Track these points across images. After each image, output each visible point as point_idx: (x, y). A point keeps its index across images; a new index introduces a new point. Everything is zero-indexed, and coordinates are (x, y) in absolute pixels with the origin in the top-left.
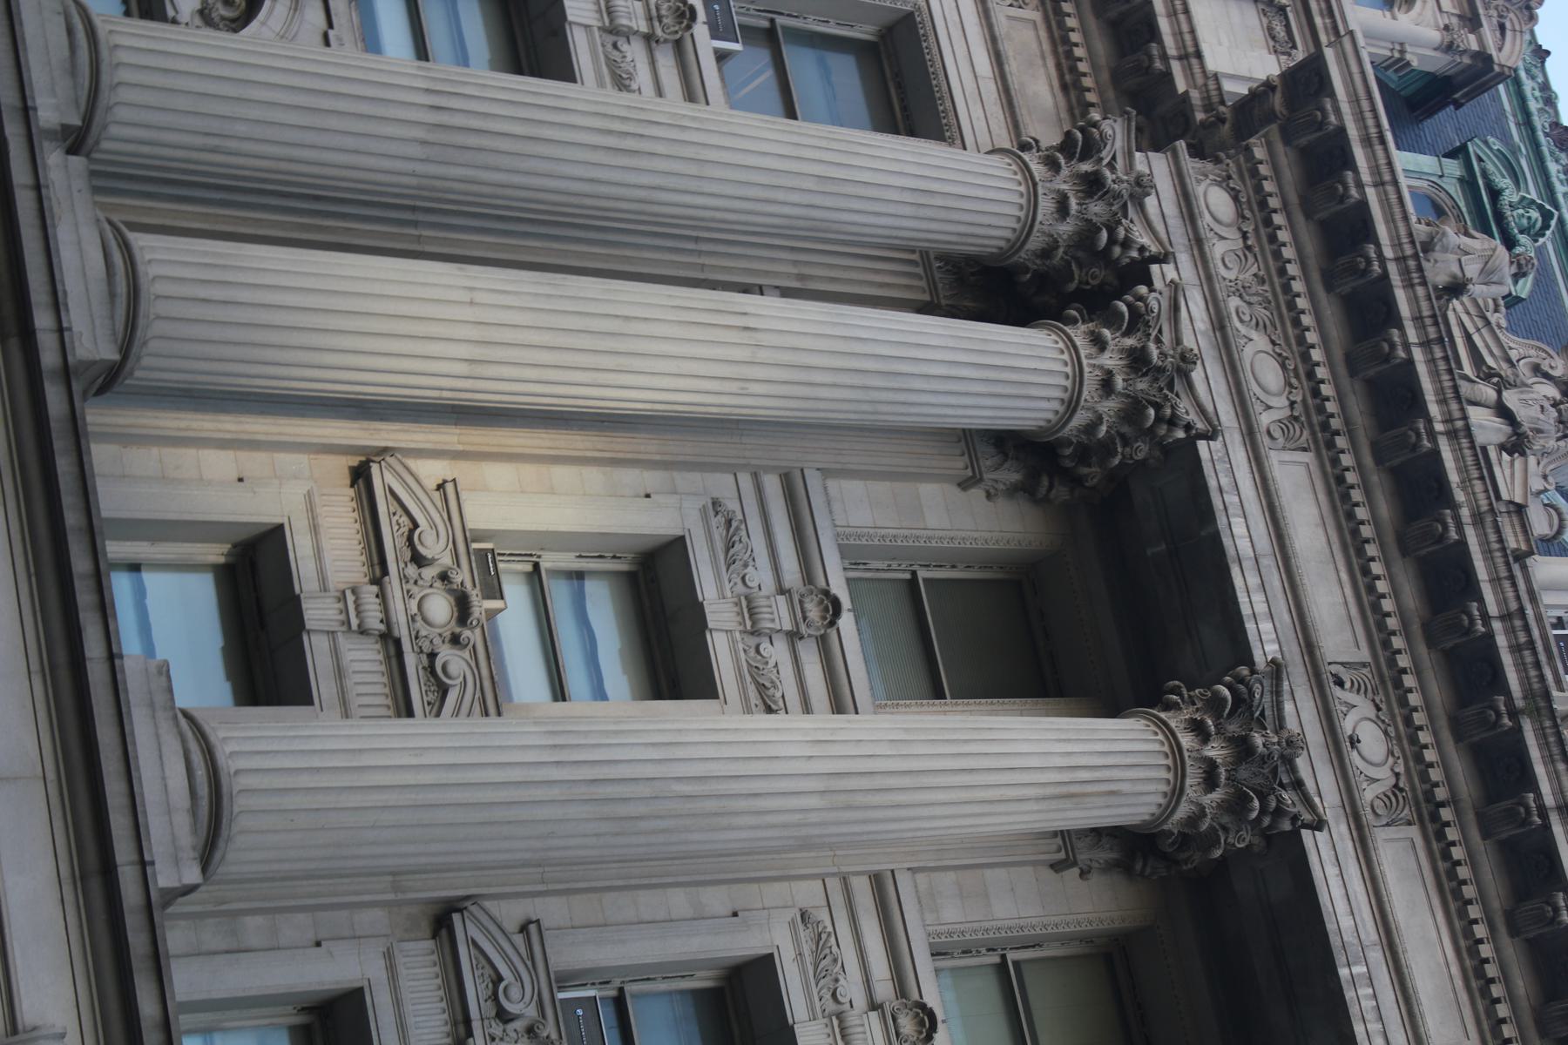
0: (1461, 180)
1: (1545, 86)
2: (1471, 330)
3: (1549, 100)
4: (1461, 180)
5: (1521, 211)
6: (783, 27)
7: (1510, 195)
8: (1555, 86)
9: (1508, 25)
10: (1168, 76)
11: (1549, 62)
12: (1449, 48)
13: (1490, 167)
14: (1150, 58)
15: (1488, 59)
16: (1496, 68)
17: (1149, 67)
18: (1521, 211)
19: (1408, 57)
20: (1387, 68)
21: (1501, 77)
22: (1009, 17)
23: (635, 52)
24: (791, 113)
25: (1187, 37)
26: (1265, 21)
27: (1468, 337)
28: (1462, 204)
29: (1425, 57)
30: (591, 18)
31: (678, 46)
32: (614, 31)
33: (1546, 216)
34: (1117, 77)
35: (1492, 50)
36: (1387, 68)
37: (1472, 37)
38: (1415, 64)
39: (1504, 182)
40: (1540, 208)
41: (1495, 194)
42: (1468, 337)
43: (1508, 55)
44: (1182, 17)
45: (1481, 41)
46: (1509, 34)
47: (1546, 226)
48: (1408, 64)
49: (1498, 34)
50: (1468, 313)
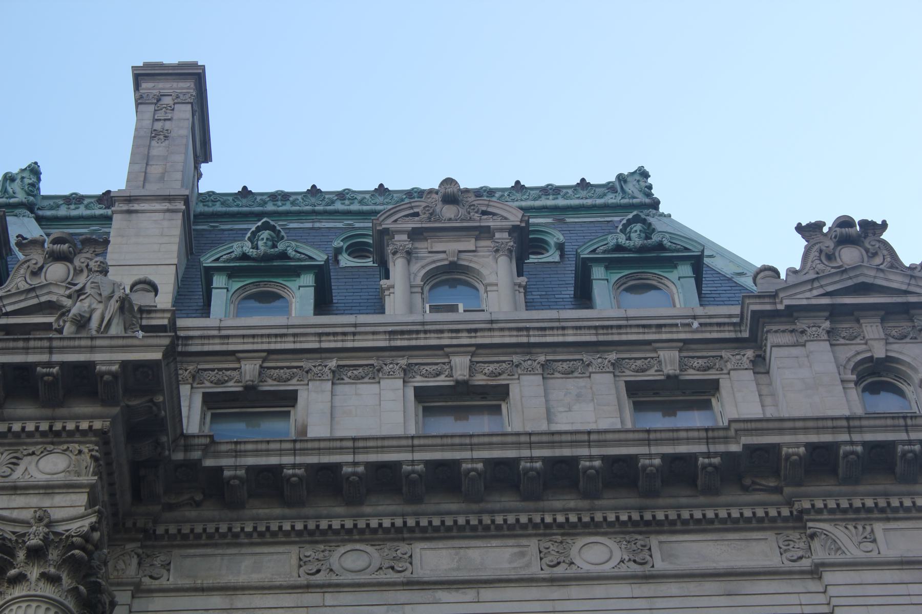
25: (696, 434)
26: (557, 375)
39: (611, 240)
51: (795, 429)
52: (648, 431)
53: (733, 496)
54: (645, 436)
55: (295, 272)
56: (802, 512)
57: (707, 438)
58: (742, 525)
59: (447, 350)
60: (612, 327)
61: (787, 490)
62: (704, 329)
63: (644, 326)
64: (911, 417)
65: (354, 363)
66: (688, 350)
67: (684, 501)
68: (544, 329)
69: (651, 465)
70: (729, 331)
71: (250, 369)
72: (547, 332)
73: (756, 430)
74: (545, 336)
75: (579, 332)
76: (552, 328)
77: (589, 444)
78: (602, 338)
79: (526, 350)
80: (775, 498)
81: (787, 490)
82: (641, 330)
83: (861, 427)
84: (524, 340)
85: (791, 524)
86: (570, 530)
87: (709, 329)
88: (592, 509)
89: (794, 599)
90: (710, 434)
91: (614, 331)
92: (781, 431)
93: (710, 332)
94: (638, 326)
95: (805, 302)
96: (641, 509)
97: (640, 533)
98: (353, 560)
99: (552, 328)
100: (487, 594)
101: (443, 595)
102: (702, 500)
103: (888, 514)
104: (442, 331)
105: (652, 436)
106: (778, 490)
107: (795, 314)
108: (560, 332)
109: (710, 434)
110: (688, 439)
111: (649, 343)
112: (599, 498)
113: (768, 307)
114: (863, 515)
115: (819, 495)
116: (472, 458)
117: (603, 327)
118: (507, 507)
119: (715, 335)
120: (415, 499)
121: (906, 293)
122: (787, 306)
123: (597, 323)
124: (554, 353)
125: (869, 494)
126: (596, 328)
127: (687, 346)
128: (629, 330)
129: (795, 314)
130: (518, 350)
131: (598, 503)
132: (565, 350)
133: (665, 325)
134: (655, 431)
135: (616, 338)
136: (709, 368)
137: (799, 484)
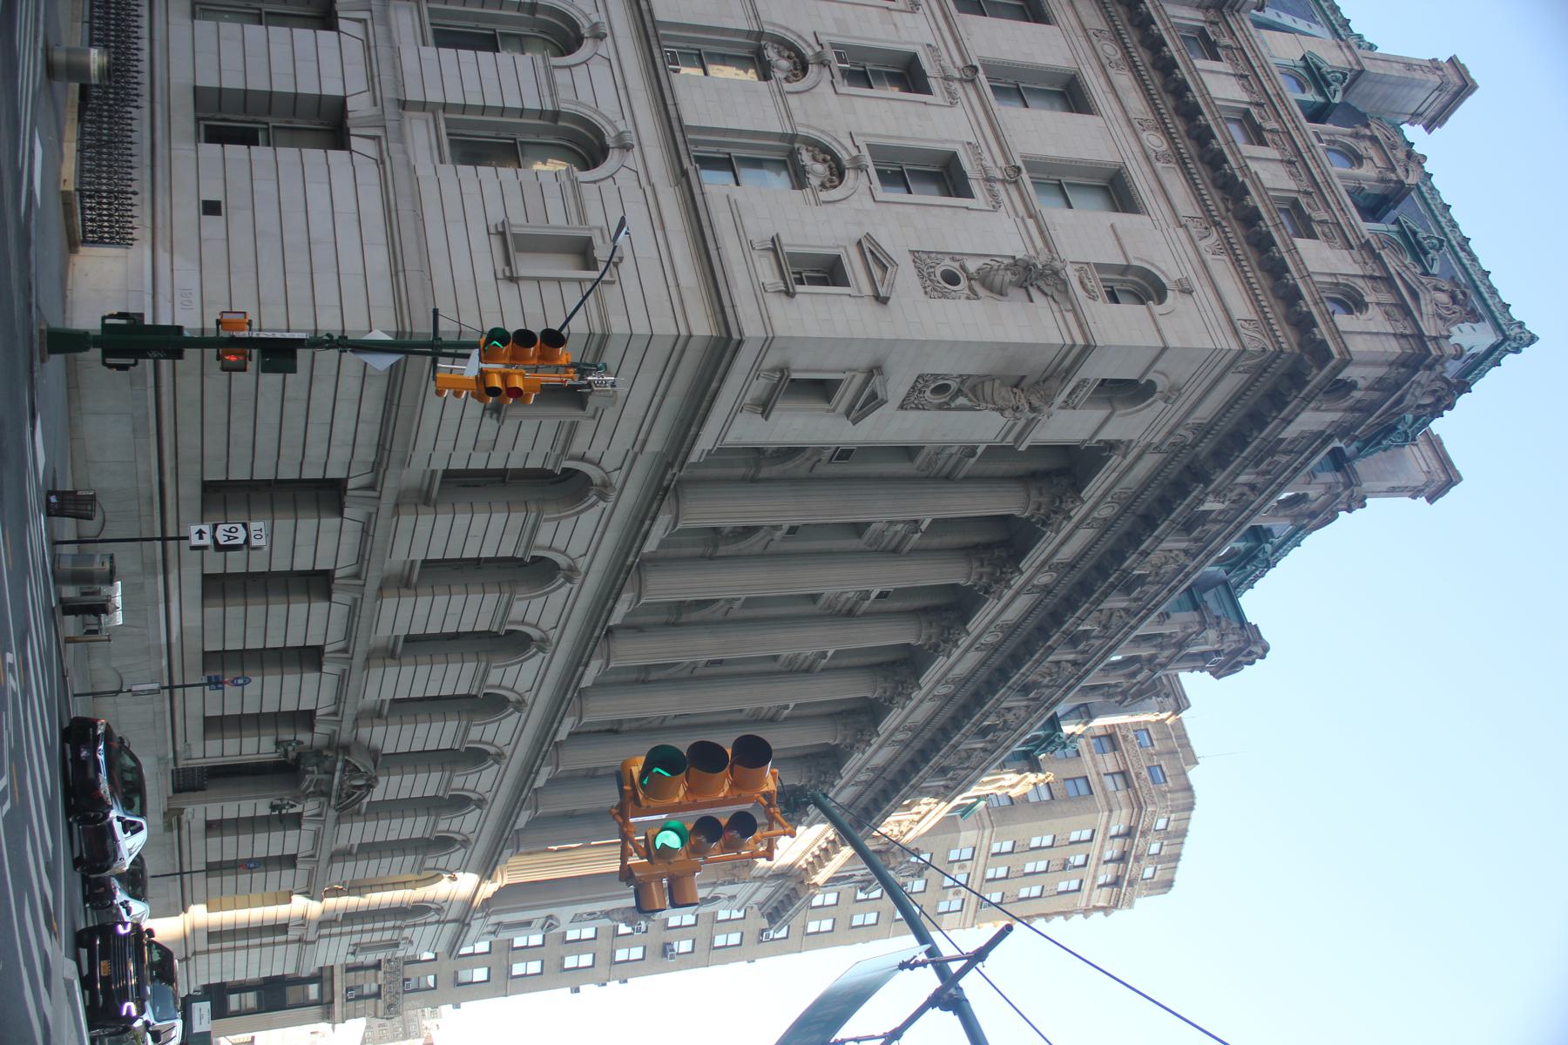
1: (1451, 220)
3: (1455, 226)
7: (1421, 234)
10: (1234, 176)
12: (1382, 180)
15: (1402, 183)
23: (998, 187)
24: (1070, 207)
30: (978, 176)
31: (1016, 182)
32: (989, 180)
33: (1441, 242)
34: (1214, 181)
41: (1415, 234)
43: (1412, 180)
47: (1442, 245)
53: (1217, 195)
55: (1321, 93)
65: (1295, 160)
71: (1271, 124)
77: (1200, 90)
86: (1133, 67)
92: (1326, 322)
98: (1110, 50)
100: (1111, 96)
101: (1102, 80)
103: (1236, 262)
106: (1228, 210)
115: (1235, 232)
116: (1219, 142)
118: (1155, 80)
120: (1201, 158)
137: (1236, 218)
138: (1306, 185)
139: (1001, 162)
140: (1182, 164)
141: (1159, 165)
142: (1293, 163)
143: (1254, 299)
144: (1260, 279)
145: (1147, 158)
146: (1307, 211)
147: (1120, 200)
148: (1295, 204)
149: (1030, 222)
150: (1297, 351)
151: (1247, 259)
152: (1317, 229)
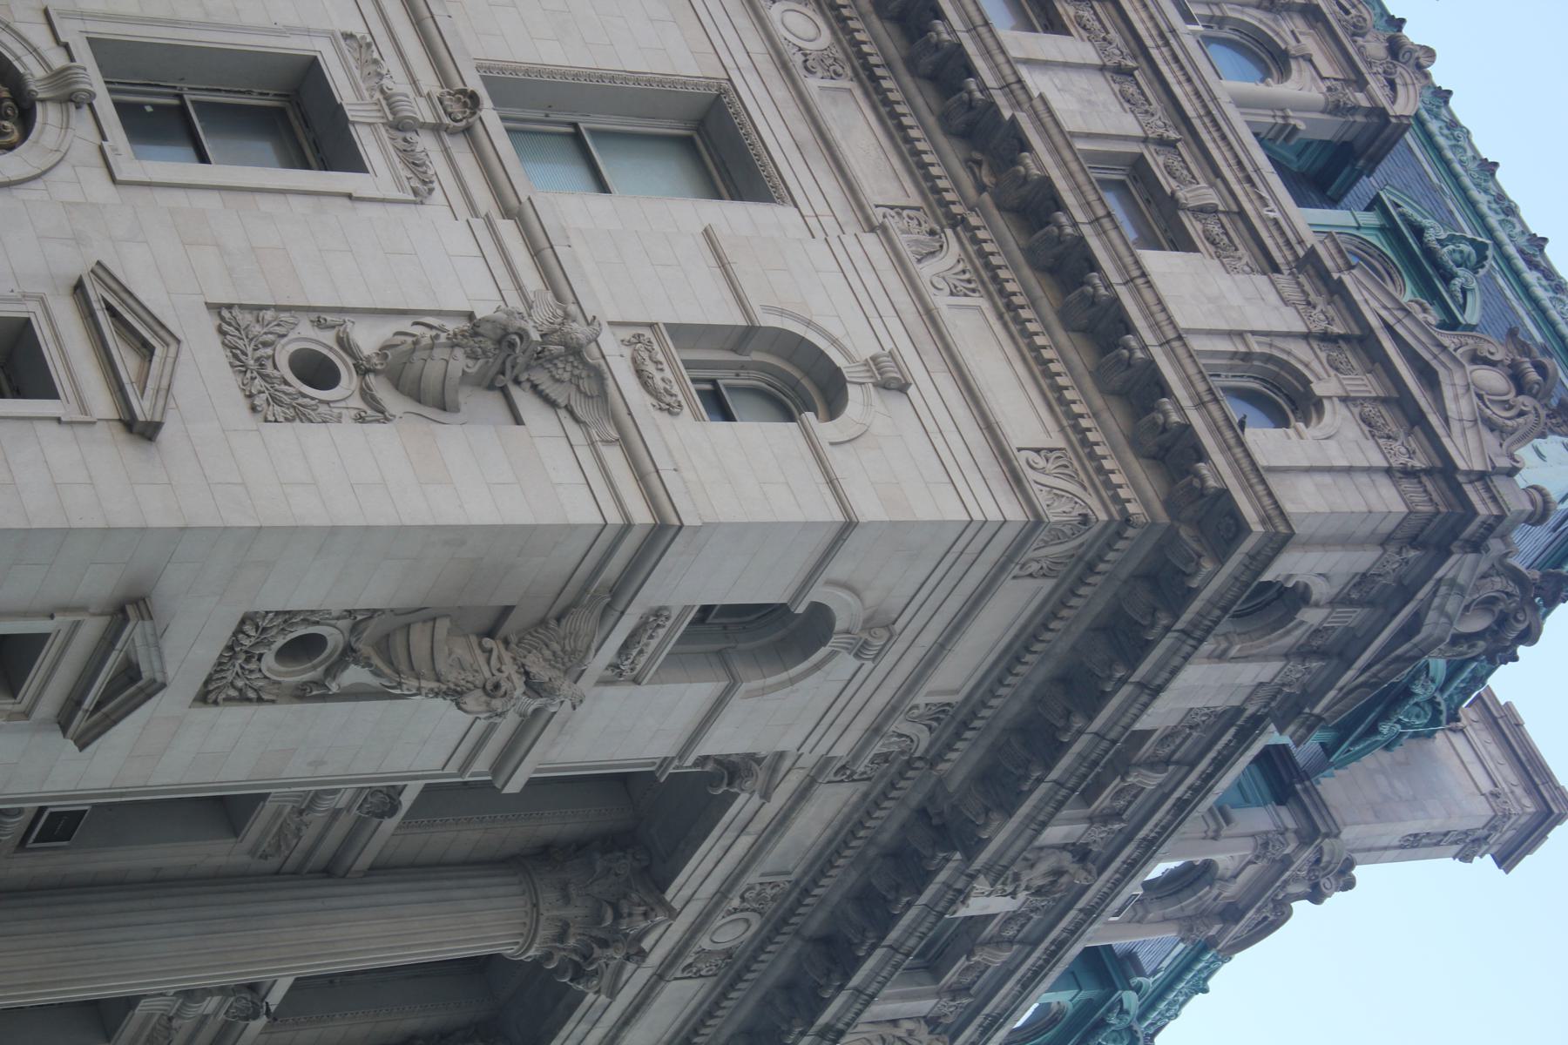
0: (1382, 229)
1: (1501, 197)
2: (1391, 320)
3: (1510, 211)
4: (1382, 229)
5: (1451, 247)
6: (588, 130)
8: (1512, 194)
9: (1398, 81)
10: (991, 105)
11: (1499, 174)
12: (1336, 109)
13: (1407, 209)
14: (970, 93)
15: (1382, 113)
16: (1394, 120)
17: (971, 100)
18: (1451, 247)
19: (1292, 122)
20: (1273, 140)
21: (1402, 129)
22: (822, 88)
27: (1389, 328)
28: (1389, 252)
29: (1314, 126)
33: (1481, 249)
35: (1384, 101)
36: (1273, 140)
37: (1360, 96)
38: (1302, 126)
40: (1472, 242)
41: (1419, 231)
42: (1389, 328)
43: (1404, 105)
44: (982, 30)
45: (1370, 98)
46: (1400, 88)
47: (1482, 257)
48: (1295, 129)
49: (1387, 89)
50: (1385, 308)
51: (1065, 164)
52: (986, 23)
54: (978, 20)
56: (964, 220)
57: (1008, 85)
58: (883, 110)
59: (1219, 182)
60: (1219, 129)
61: (986, 196)
62: (1273, 228)
63: (1239, 163)
64: (1148, 282)
66: (1233, 223)
67: (919, 101)
68: (1176, 59)
69: (938, 34)
70: (1284, 257)
72: (1174, 66)
73: (1043, 125)
74: (1168, 64)
75: (1193, 98)
76: (1182, 68)
78: (1197, 123)
79: (1137, 52)
80: (971, 192)
81: (986, 196)
82: (1232, 162)
83: (1105, 232)
84: (1149, 42)
85: (856, 64)
87: (1276, 234)
88: (862, 16)
89: (821, 208)
90: (1015, 87)
91: (1216, 135)
92: (1226, 448)
93: (1272, 236)
94: (1236, 156)
95: (1357, 297)
96: (888, 65)
97: (856, 75)
99: (1182, 68)
102: (931, 121)
103: (1008, 311)
104: (1189, 80)
105: (982, 30)
106: (981, 188)
107: (1336, 297)
108: (1182, 78)
109: (1015, 87)
110: (997, 66)
111: (1218, 173)
112: (880, 18)
113: (1329, 263)
114: (985, 275)
115: (1001, 237)
117: (1214, 121)
119: (1269, 242)
120: (911, 64)
121: (1446, 420)
122: (1340, 281)
123: (1215, 112)
124: (1150, 83)
125: (1023, 284)
126: (1209, 113)
127: (1237, 218)
128: (1224, 149)
129: (1336, 297)
130: (1129, 37)
131: (874, 19)
132: (1160, 91)
133: (1253, 185)
134: (990, 30)
135: (1205, 136)
136: (1213, 243)
137: (999, 207)
138: (1160, 124)
139: (429, 82)
140: (868, 79)
141: (812, 84)
142: (1129, 73)
143: (1055, 399)
144: (1068, 354)
145: (784, 66)
146: (1168, 184)
147: (722, 167)
148: (1138, 166)
149: (507, 228)
150: (1163, 518)
151: (1033, 304)
152: (1194, 227)
